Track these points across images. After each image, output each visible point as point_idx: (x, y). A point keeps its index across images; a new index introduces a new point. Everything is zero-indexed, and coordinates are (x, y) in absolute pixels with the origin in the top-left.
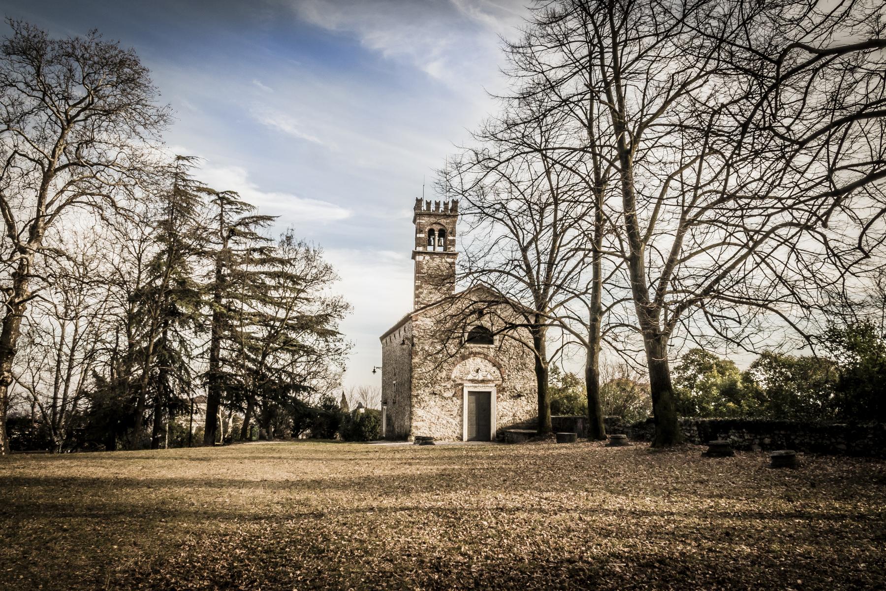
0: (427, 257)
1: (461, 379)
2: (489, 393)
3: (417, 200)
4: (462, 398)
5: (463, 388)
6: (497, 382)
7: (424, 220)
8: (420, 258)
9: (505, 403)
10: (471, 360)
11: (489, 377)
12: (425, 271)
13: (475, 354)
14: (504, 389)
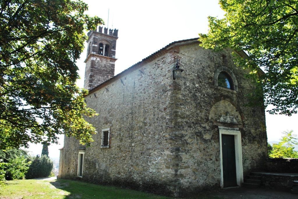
0: (98, 59)
4: (219, 142)
6: (240, 126)
7: (98, 37)
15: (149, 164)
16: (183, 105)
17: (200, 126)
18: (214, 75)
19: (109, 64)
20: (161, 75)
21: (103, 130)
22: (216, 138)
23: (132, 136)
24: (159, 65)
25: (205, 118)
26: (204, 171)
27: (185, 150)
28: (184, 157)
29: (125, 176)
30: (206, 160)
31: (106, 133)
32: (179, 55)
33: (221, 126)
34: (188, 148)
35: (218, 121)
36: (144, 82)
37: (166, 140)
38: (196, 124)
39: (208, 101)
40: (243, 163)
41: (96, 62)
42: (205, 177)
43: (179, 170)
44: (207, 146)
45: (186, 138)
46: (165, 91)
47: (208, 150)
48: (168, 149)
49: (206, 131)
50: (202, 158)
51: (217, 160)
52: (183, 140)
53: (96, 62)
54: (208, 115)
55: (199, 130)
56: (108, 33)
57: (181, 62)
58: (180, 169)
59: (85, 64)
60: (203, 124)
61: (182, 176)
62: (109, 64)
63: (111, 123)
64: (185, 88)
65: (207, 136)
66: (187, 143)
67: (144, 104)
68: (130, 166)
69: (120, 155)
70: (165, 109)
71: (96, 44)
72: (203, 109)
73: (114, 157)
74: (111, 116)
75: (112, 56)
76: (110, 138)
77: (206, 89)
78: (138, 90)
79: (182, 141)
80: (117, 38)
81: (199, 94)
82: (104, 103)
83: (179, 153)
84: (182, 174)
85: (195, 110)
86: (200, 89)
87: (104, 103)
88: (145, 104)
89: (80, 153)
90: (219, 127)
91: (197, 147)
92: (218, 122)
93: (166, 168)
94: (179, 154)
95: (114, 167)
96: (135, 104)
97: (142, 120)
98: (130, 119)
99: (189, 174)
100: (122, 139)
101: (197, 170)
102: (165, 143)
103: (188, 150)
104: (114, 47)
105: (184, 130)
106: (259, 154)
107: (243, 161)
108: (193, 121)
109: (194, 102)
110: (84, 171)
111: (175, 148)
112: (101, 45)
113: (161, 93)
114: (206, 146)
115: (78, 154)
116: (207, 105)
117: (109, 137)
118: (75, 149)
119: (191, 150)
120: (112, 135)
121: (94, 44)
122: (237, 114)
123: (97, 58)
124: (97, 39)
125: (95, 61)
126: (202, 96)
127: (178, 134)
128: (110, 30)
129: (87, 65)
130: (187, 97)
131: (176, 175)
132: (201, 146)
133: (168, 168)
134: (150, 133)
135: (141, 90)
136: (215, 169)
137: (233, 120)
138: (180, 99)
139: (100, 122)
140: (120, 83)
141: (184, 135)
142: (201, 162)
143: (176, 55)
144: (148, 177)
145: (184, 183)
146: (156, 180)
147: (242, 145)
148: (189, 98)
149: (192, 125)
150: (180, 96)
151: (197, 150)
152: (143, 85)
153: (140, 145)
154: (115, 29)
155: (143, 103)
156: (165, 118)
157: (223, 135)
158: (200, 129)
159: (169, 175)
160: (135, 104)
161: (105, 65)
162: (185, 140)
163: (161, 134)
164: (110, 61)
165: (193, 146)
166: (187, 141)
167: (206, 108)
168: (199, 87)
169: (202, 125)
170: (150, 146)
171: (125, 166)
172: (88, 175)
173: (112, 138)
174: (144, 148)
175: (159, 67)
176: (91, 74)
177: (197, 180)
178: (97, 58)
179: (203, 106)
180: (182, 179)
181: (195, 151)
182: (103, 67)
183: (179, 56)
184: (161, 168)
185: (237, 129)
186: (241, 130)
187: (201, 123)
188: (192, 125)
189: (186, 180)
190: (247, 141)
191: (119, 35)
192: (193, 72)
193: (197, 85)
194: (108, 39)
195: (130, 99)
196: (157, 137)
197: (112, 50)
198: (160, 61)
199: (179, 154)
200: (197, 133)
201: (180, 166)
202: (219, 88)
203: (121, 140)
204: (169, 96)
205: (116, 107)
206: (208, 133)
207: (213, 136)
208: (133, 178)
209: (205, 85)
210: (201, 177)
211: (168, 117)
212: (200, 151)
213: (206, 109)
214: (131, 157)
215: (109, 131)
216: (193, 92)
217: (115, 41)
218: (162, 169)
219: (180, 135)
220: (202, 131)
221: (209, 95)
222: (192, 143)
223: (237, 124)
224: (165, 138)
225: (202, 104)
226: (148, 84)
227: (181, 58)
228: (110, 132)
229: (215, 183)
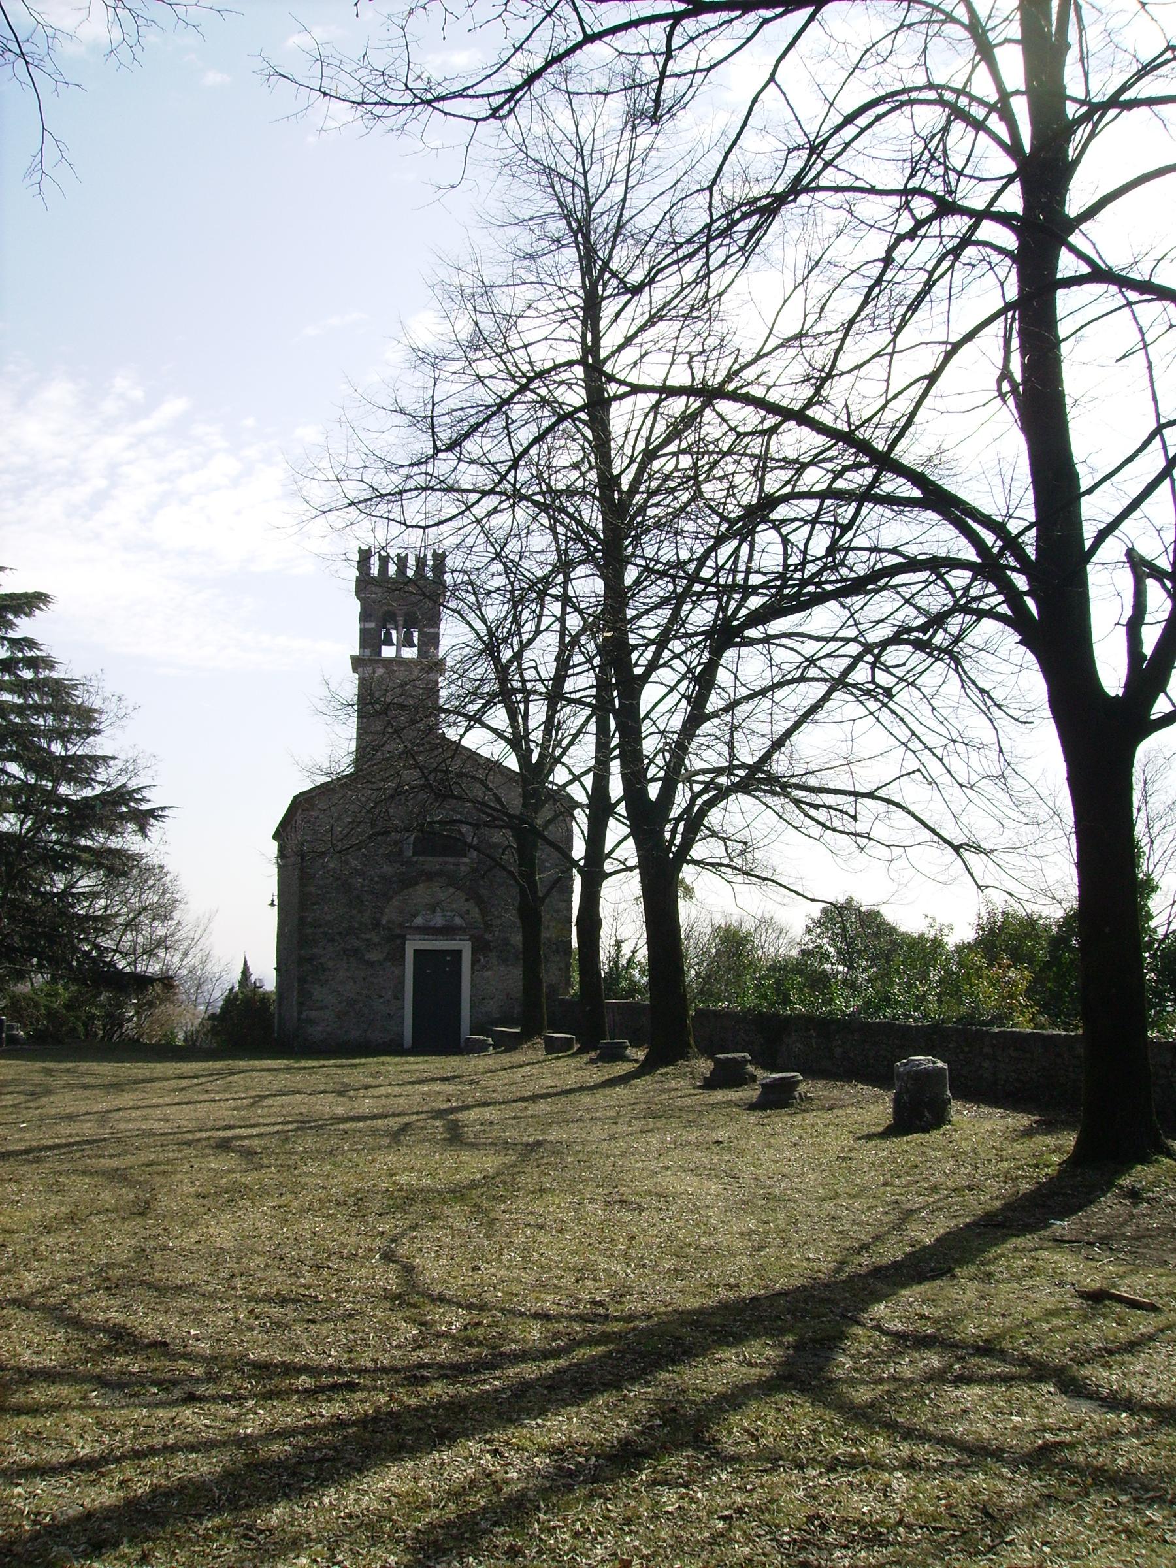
1: (401, 926)
2: (459, 953)
9: (489, 973)
10: (421, 888)
11: (458, 921)
13: (430, 876)
16: (319, 904)
28: (318, 992)
45: (323, 960)
54: (378, 915)
56: (410, 573)
61: (310, 1021)
65: (374, 956)
122: (470, 905)
149: (337, 937)
150: (313, 889)
158: (357, 943)
162: (321, 964)
186: (472, 938)
188: (337, 937)
189: (319, 1028)
202: (415, 859)
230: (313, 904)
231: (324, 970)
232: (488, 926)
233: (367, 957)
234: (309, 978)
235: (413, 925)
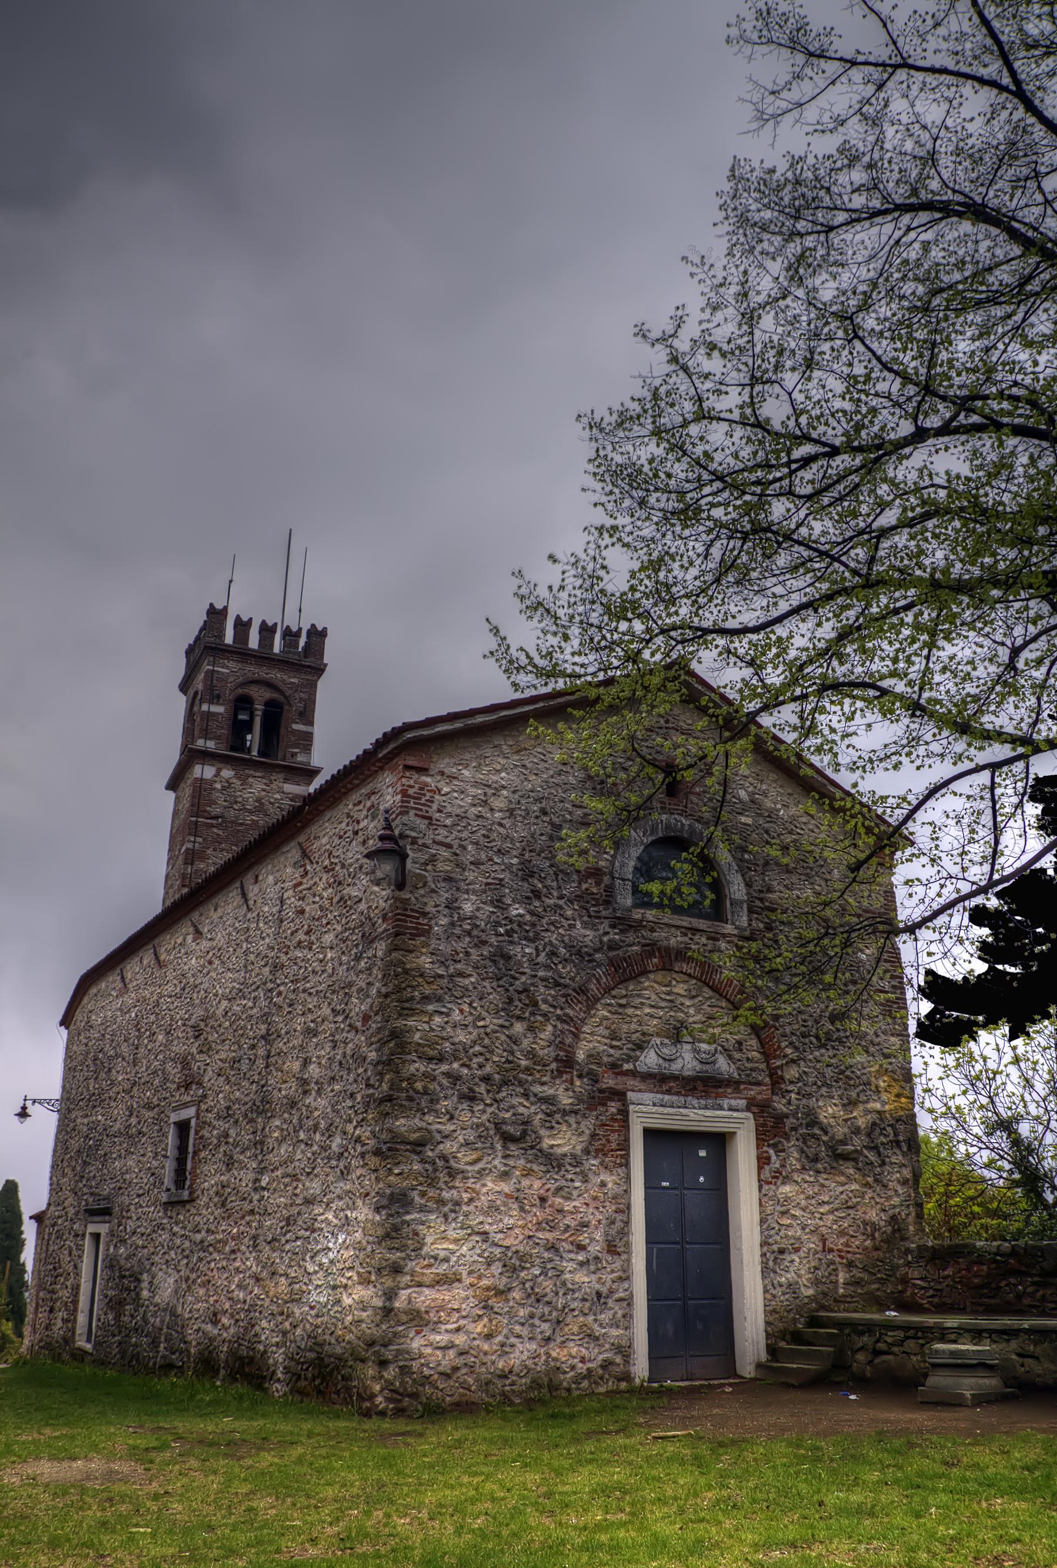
0: (227, 773)
3: (212, 611)
4: (626, 1163)
5: (624, 1113)
7: (228, 669)
8: (205, 771)
9: (787, 1189)
11: (723, 1064)
12: (216, 810)
14: (780, 1118)
15: (311, 1268)
16: (439, 1000)
17: (526, 1095)
18: (614, 857)
19: (278, 796)
20: (361, 867)
21: (174, 1117)
22: (614, 1146)
23: (262, 1143)
24: (358, 822)
25: (553, 1054)
26: (538, 1301)
27: (441, 1202)
29: (232, 1331)
30: (552, 1248)
31: (183, 1127)
32: (428, 780)
33: (640, 1091)
34: (454, 1191)
35: (626, 1067)
36: (311, 899)
37: (363, 1155)
38: (505, 1083)
39: (572, 979)
40: (766, 1271)
41: (218, 786)
42: (545, 1326)
43: (404, 1294)
44: (564, 1183)
45: (448, 1147)
46: (369, 940)
47: (568, 1206)
48: (367, 1195)
49: (558, 1117)
50: (530, 1237)
51: (611, 1249)
52: (430, 1154)
53: (218, 786)
54: (569, 1040)
55: (521, 1110)
56: (277, 646)
57: (439, 811)
58: (408, 1287)
59: (172, 795)
60: (543, 1084)
61: (418, 1319)
62: (278, 796)
63: (200, 1084)
64: (452, 924)
66: (452, 1173)
67: (305, 995)
68: (252, 1282)
69: (224, 1231)
70: (366, 1018)
71: (218, 704)
72: (544, 1015)
73: (202, 1242)
74: (201, 1052)
75: (293, 755)
76: (195, 1153)
77: (565, 923)
78: (292, 934)
79: (423, 1161)
80: (319, 670)
81: (523, 951)
82: (184, 989)
83: (408, 1213)
84: (418, 1312)
85: (501, 1022)
86: (534, 925)
87: (184, 989)
88: (310, 994)
89: (91, 1228)
90: (630, 1094)
91: (506, 1187)
92: (626, 1073)
93: (360, 1283)
94: (408, 1218)
95: (202, 1292)
96: (280, 994)
97: (296, 1066)
98: (260, 1063)
99: (458, 1310)
100: (231, 1157)
101: (501, 1293)
102: (359, 1172)
103: (457, 1204)
104: (307, 715)
105: (436, 1111)
106: (865, 1223)
107: (763, 1255)
108: (488, 1069)
109: (495, 984)
110: (99, 1320)
111: (388, 1191)
112: (243, 702)
113: (357, 946)
114: (552, 1186)
115: (84, 1235)
116: (565, 996)
117: (191, 1149)
118: (77, 1214)
119: (471, 1200)
120: (202, 1137)
121: (211, 702)
123: (219, 771)
124: (223, 679)
125: (211, 782)
126: (542, 958)
127: (403, 1129)
128: (287, 633)
129: (177, 801)
130: (459, 966)
131: (387, 1312)
132: (526, 1182)
133: (365, 1281)
134: (316, 1127)
135: (301, 936)
136: (599, 1295)
137: (714, 1062)
138: (421, 975)
139: (166, 1080)
140: (239, 900)
141: (438, 1137)
142: (522, 1257)
143: (412, 782)
144: (304, 1330)
145: (428, 1350)
146: (327, 1337)
147: (761, 1183)
148: (469, 970)
149: (482, 1089)
150: (425, 961)
151: (505, 1204)
152: (307, 909)
153: (287, 1180)
154: (313, 625)
155: (304, 991)
156: (365, 1058)
157: (649, 1133)
158: (526, 1109)
159: (365, 1314)
160: (280, 994)
161: (259, 800)
162: (444, 1158)
163: (350, 1128)
164: (286, 780)
165: (484, 1185)
166: (452, 1163)
167: (559, 1012)
168: (528, 918)
169: (537, 1089)
170: (315, 1187)
171: (236, 1279)
172: (114, 1336)
173: (202, 1155)
174: (296, 1195)
175: (356, 833)
176: (190, 846)
177: (500, 1338)
178: (219, 771)
179: (545, 1001)
180: (418, 1333)
181: (493, 1209)
182: (251, 812)
183: (426, 784)
184: (344, 1281)
185: (734, 1102)
186: (759, 1108)
187: (530, 1078)
188: (482, 1089)
190: (794, 1160)
191: (330, 655)
192: (499, 851)
193: (517, 910)
194: (276, 675)
195: (267, 969)
196: (336, 1143)
197: (295, 726)
198: (361, 807)
199: (408, 1218)
200: (504, 1122)
201: (413, 1273)
202: (637, 914)
203: (230, 1163)
204: (379, 963)
205: (220, 1012)
206: (570, 1125)
207: (593, 1136)
208: (256, 1335)
209: (561, 908)
210: (523, 1324)
211: (372, 1055)
212: (522, 1209)
213: (559, 1018)
214: (255, 1238)
215: (193, 1122)
216: (493, 940)
217: (313, 686)
218: (346, 1287)
219: (414, 1136)
220: (536, 1114)
221: (579, 953)
222: (479, 1172)
223: (738, 1083)
224: (359, 1149)
225: (542, 992)
226: (321, 908)
227: (439, 791)
228: (197, 1125)
229: (601, 1357)
230: (426, 999)
231: (452, 1173)
232: (776, 1081)
233: (547, 1142)
234: (415, 1195)
235: (641, 1068)
